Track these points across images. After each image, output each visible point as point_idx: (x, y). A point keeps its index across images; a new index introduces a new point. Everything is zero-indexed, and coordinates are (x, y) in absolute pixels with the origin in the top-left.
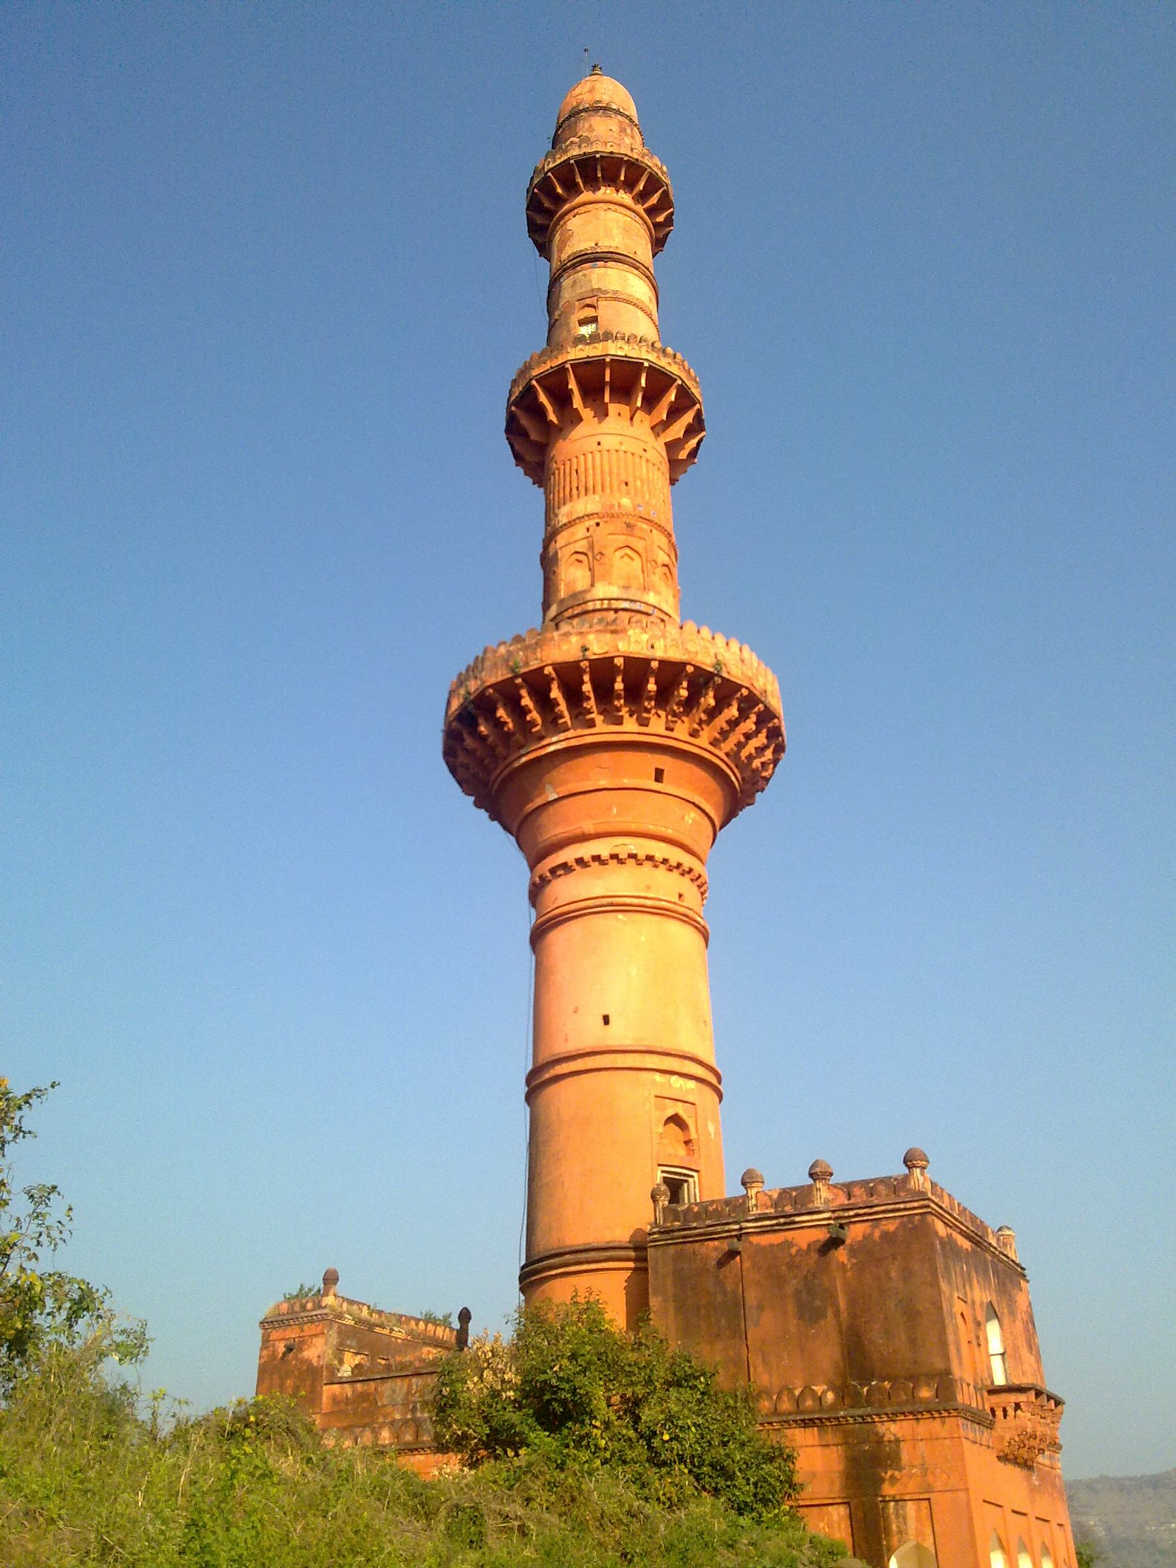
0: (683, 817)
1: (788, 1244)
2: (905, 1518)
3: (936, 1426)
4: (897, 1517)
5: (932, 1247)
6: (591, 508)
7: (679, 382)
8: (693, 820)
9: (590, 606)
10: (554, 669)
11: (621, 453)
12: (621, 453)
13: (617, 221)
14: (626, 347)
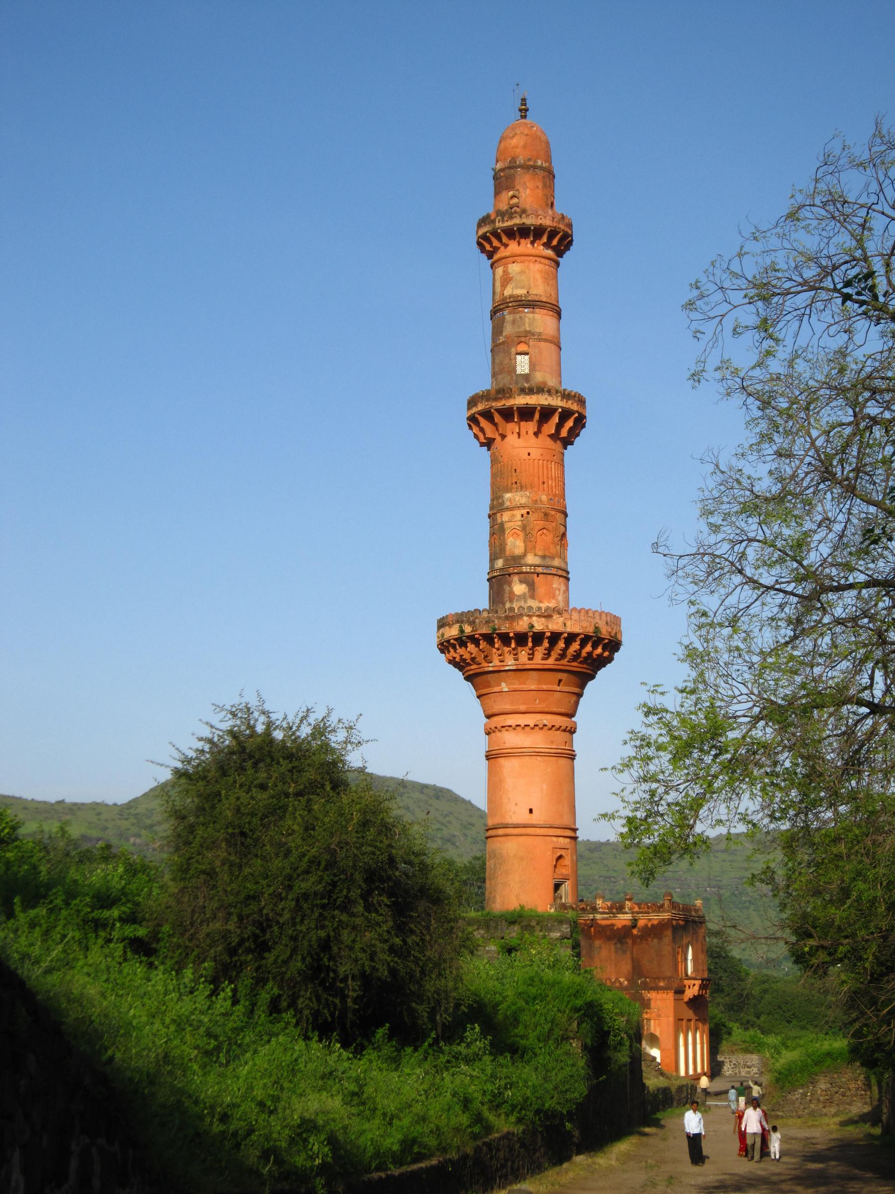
1: (613, 925)
6: (524, 501)
9: (524, 569)
13: (540, 272)
14: (550, 398)
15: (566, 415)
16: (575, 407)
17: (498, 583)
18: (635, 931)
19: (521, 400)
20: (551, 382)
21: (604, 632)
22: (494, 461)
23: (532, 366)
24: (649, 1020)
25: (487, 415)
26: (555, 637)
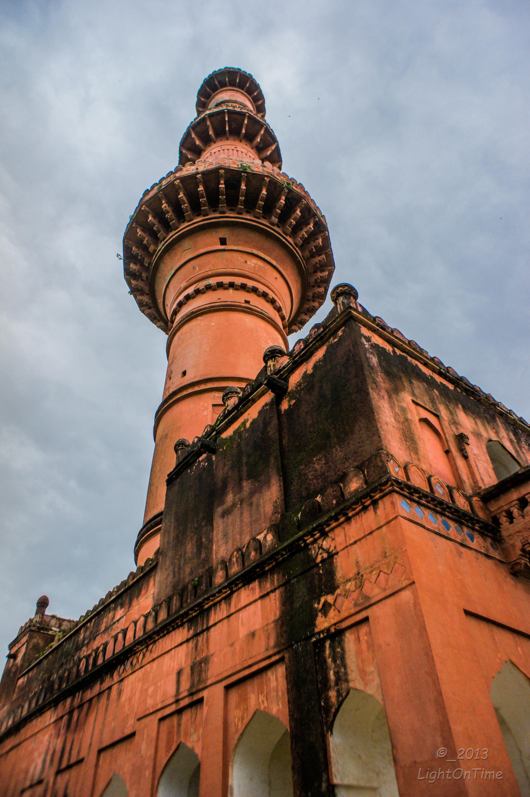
0: (246, 262)
2: (343, 658)
3: (368, 519)
4: (334, 661)
5: (357, 344)
7: (247, 114)
8: (255, 264)
10: (147, 206)
11: (221, 151)
12: (221, 151)
18: (285, 406)
24: (336, 635)
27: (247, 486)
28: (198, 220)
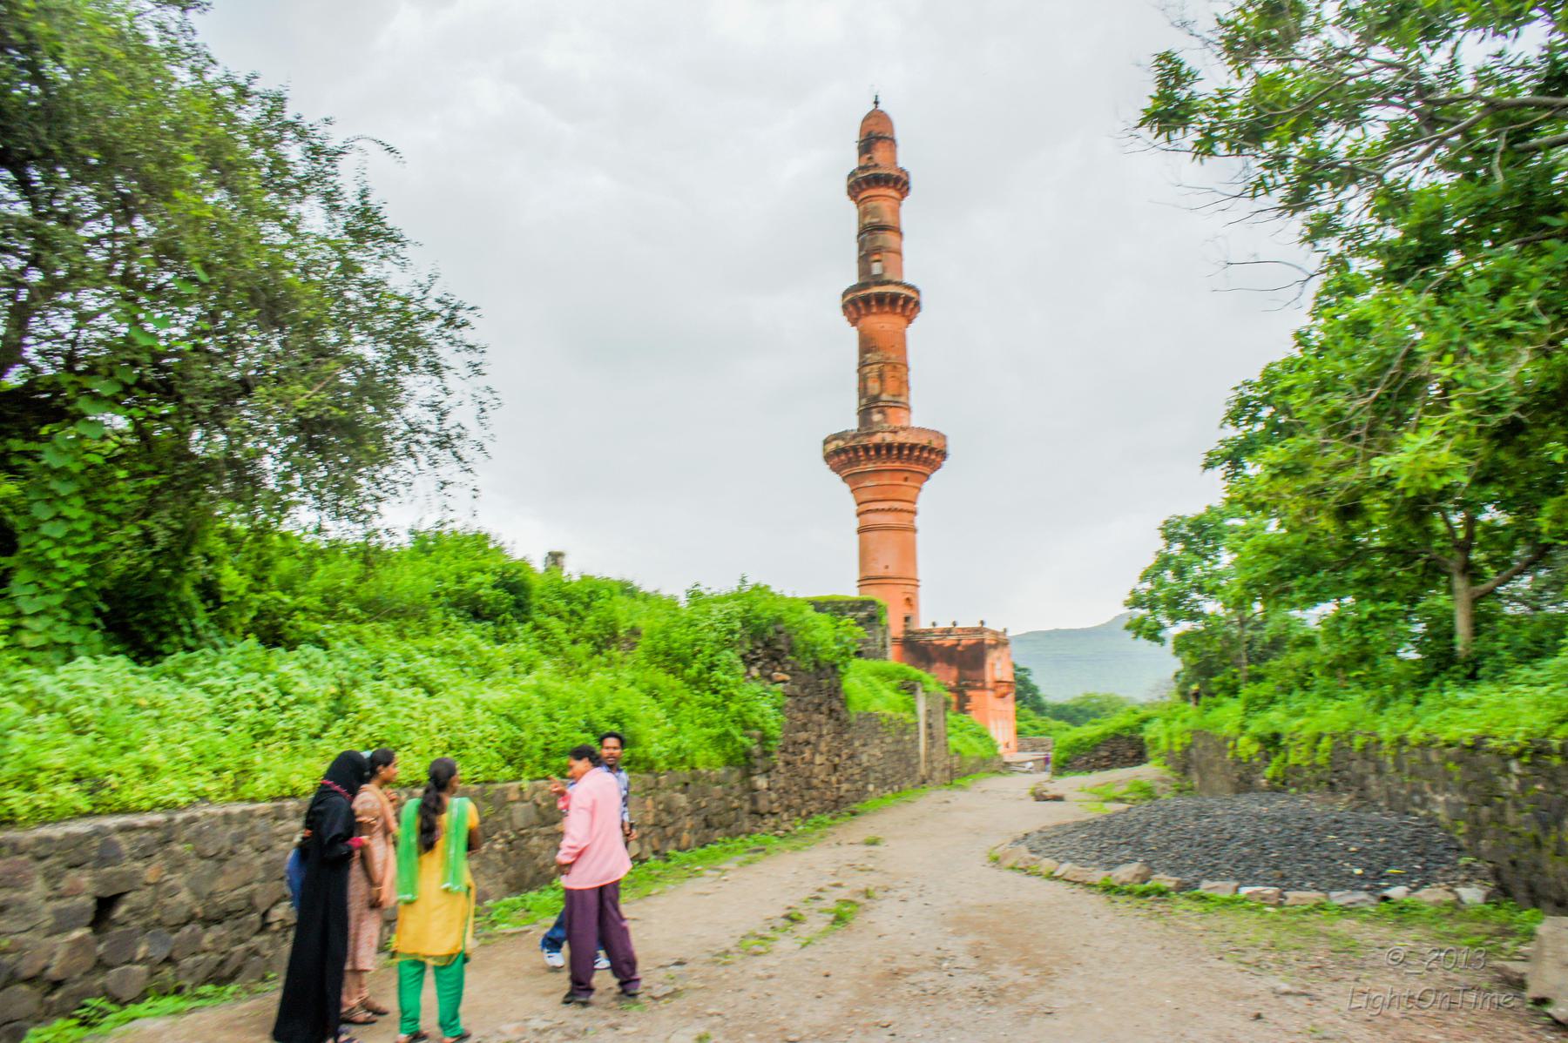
15: (908, 300)
16: (913, 295)
17: (864, 414)
19: (876, 290)
20: (897, 279)
21: (935, 444)
22: (861, 333)
23: (884, 269)
25: (853, 302)
26: (901, 447)
27: (945, 665)
28: (897, 465)
